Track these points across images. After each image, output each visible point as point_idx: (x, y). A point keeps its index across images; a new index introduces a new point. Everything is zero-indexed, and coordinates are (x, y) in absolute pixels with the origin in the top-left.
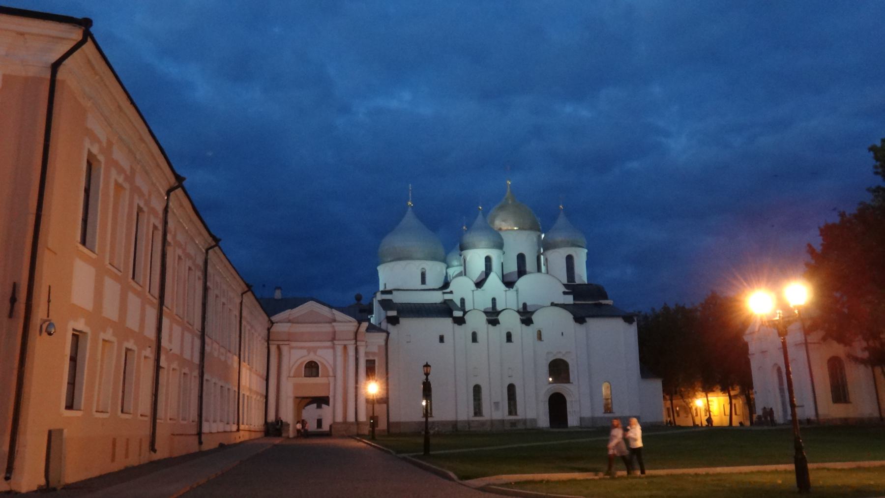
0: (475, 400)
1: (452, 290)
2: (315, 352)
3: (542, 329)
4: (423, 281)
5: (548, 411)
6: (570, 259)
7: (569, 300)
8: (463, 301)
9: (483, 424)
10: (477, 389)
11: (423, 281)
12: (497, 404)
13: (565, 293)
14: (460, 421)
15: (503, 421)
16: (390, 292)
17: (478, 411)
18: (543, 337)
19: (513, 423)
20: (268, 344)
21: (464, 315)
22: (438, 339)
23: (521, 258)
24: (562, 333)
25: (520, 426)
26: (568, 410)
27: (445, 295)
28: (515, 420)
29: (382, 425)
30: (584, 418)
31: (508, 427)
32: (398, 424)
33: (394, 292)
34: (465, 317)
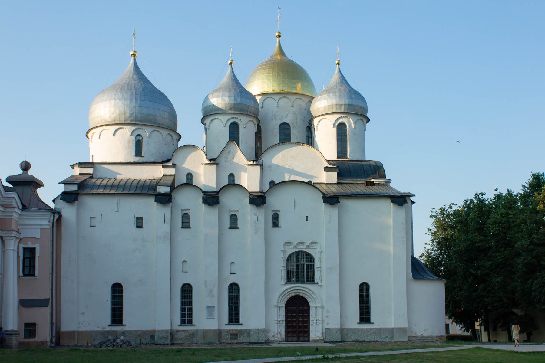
0: (183, 303)
1: (175, 163)
3: (279, 211)
4: (139, 152)
5: (284, 319)
6: (341, 128)
12: (210, 309)
13: (326, 169)
14: (159, 331)
16: (92, 165)
18: (281, 222)
19: (234, 335)
24: (307, 217)
25: (242, 339)
26: (311, 319)
28: (236, 330)
33: (97, 166)
34: (172, 194)
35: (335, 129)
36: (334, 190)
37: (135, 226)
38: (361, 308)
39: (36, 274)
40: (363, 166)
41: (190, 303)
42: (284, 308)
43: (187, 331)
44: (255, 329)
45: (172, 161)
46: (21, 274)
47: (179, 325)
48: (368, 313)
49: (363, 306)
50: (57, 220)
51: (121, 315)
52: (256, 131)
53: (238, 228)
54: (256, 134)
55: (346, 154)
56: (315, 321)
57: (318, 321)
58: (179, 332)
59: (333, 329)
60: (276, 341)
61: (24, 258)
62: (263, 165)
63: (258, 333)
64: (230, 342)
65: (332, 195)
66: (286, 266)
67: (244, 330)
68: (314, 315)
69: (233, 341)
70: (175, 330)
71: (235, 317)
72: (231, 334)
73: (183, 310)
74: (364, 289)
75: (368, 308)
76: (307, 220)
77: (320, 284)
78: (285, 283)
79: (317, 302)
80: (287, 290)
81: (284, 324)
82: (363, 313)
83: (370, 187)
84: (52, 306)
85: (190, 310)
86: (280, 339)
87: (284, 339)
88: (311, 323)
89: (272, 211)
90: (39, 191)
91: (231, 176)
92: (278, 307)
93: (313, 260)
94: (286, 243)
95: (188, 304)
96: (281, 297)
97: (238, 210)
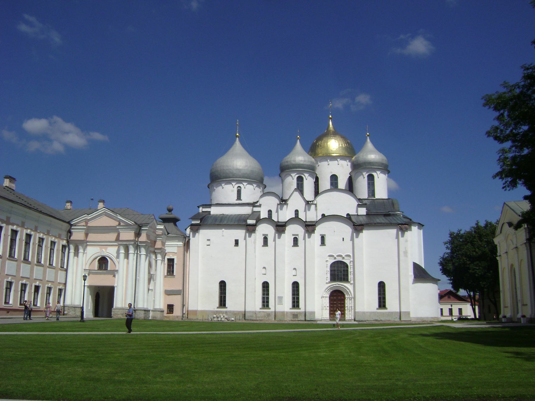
0: (263, 294)
2: (106, 249)
3: (325, 235)
4: (239, 197)
5: (328, 305)
7: (363, 211)
8: (270, 212)
9: (269, 315)
10: (266, 286)
11: (239, 197)
13: (359, 206)
14: (248, 311)
15: (287, 312)
17: (265, 303)
19: (295, 316)
20: (68, 242)
21: (257, 222)
22: (234, 242)
23: (334, 179)
24: (343, 238)
26: (346, 305)
27: (254, 208)
28: (297, 312)
29: (177, 312)
30: (358, 312)
31: (288, 319)
32: (195, 312)
35: (366, 178)
36: (363, 220)
37: (234, 245)
38: (380, 299)
39: (174, 275)
40: (384, 202)
41: (268, 294)
42: (328, 298)
43: (266, 312)
44: (309, 312)
45: (259, 202)
46: (166, 275)
47: (260, 309)
48: (384, 302)
49: (381, 297)
50: (187, 241)
51: (225, 301)
52: (315, 181)
53: (298, 246)
54: (315, 182)
55: (373, 195)
56: (349, 307)
57: (351, 307)
58: (261, 313)
59: (360, 312)
60: (323, 320)
61: (168, 265)
62: (317, 204)
63: (311, 314)
64: (293, 320)
65: (360, 223)
66: (329, 270)
67: (302, 312)
68: (348, 303)
69: (295, 319)
70: (258, 312)
71: (296, 303)
72: (293, 315)
73: (263, 298)
74: (382, 286)
75: (384, 298)
76: (343, 240)
77: (352, 282)
78: (329, 282)
79: (350, 294)
80: (331, 286)
81: (328, 308)
82: (381, 302)
83: (388, 218)
84: (183, 294)
85: (268, 298)
86: (325, 318)
87: (329, 318)
88: (346, 308)
89: (320, 235)
90: (177, 223)
91: (297, 212)
92: (324, 297)
93: (347, 266)
94: (330, 256)
95: (266, 294)
96: (326, 291)
97: (298, 235)
